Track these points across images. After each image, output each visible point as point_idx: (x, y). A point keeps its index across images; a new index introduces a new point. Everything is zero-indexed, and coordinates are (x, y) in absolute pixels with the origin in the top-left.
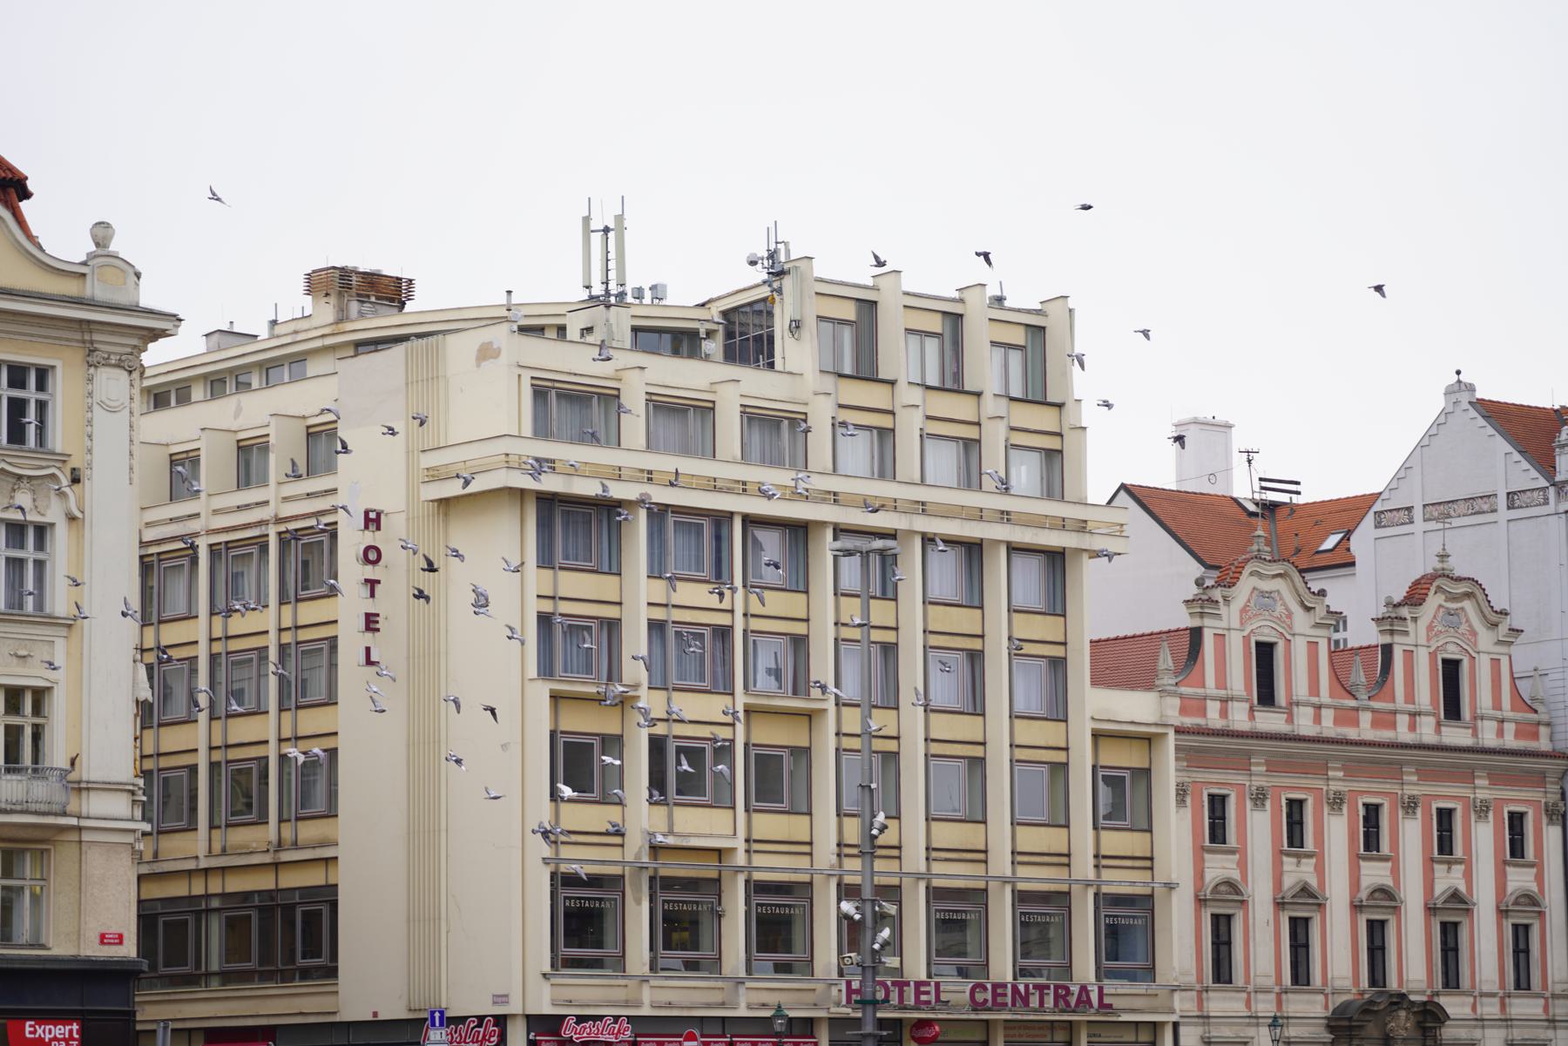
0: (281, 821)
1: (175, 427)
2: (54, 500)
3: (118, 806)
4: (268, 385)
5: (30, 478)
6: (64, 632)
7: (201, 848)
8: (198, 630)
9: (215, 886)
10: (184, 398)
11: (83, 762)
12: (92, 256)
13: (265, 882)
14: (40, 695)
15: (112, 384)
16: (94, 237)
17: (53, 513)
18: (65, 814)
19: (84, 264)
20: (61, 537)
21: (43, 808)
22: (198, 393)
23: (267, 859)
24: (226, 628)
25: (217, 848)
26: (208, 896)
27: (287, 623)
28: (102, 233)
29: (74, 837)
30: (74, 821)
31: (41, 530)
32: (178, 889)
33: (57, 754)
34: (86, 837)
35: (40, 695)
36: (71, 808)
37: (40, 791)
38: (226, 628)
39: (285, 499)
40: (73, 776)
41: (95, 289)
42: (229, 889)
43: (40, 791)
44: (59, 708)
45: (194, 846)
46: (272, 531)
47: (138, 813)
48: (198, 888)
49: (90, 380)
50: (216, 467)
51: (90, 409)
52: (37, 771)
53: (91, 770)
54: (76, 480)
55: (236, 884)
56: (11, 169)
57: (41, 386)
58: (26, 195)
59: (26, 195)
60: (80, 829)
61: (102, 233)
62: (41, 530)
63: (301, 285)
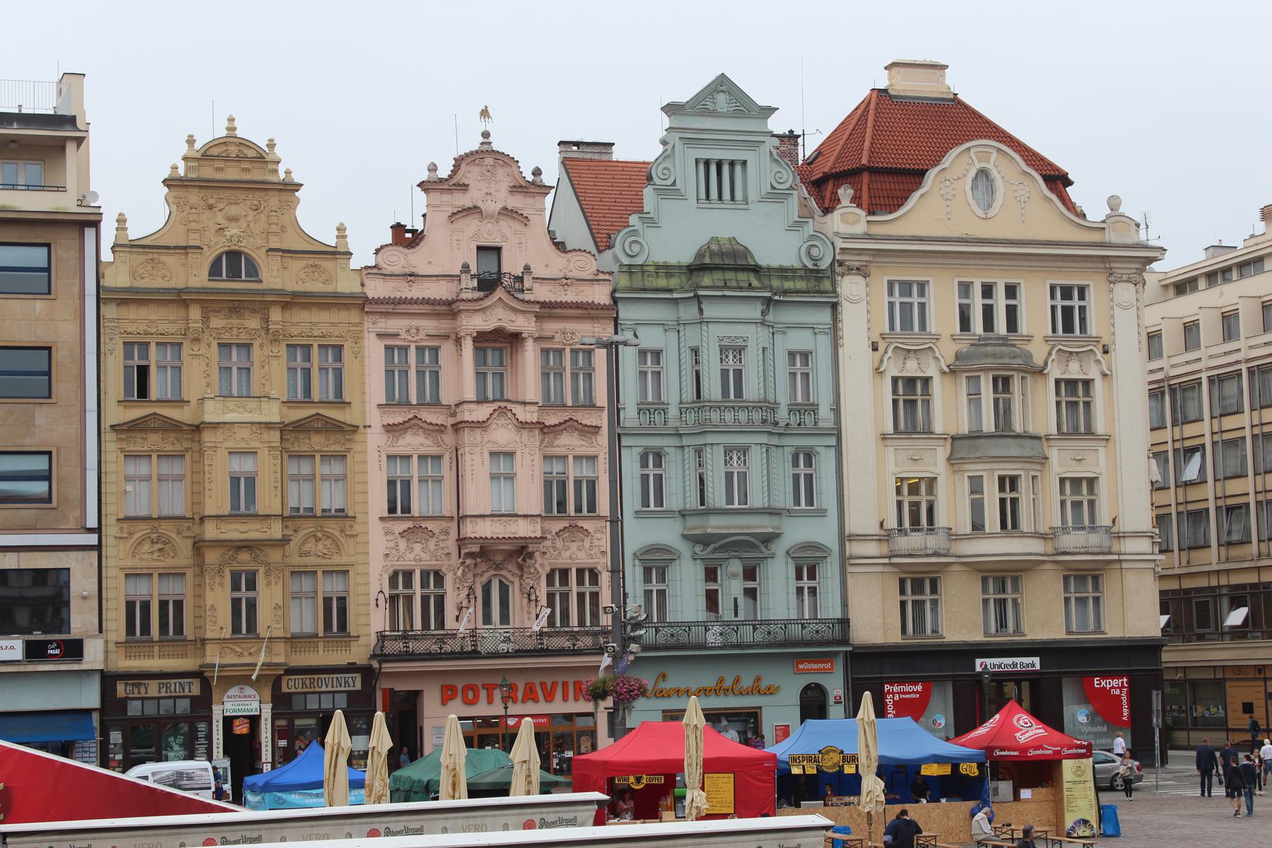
0: (1259, 541)
1: (1187, 306)
2: (1093, 365)
3: (1144, 545)
4: (1242, 276)
5: (1077, 353)
6: (1104, 443)
7: (1215, 559)
8: (1205, 427)
9: (1224, 581)
10: (1195, 289)
11: (1120, 521)
12: (1109, 217)
13: (1252, 578)
14: (1092, 481)
15: (1124, 292)
16: (1109, 205)
17: (1093, 373)
18: (1110, 553)
19: (1104, 222)
20: (1098, 388)
21: (1098, 550)
22: (1202, 284)
23: (1252, 564)
24: (1220, 426)
25: (1223, 558)
26: (1219, 587)
27: (1256, 422)
28: (1114, 203)
29: (1117, 566)
30: (1116, 557)
31: (1087, 383)
32: (1202, 583)
33: (1104, 519)
34: (1125, 565)
35: (1092, 481)
36: (1115, 549)
37: (1095, 540)
38: (1220, 426)
39: (1251, 347)
40: (1115, 529)
41: (1111, 236)
42: (1232, 583)
43: (1095, 540)
44: (1103, 488)
45: (1211, 558)
46: (1244, 367)
47: (1157, 550)
48: (1214, 583)
49: (1111, 291)
50: (1210, 330)
51: (1112, 308)
52: (1093, 529)
53: (1125, 525)
54: (1106, 352)
55: (1236, 580)
56: (1058, 169)
57: (1082, 297)
58: (1070, 183)
59: (1070, 183)
60: (1120, 561)
61: (1114, 203)
62: (1087, 383)
63: (1258, 215)
